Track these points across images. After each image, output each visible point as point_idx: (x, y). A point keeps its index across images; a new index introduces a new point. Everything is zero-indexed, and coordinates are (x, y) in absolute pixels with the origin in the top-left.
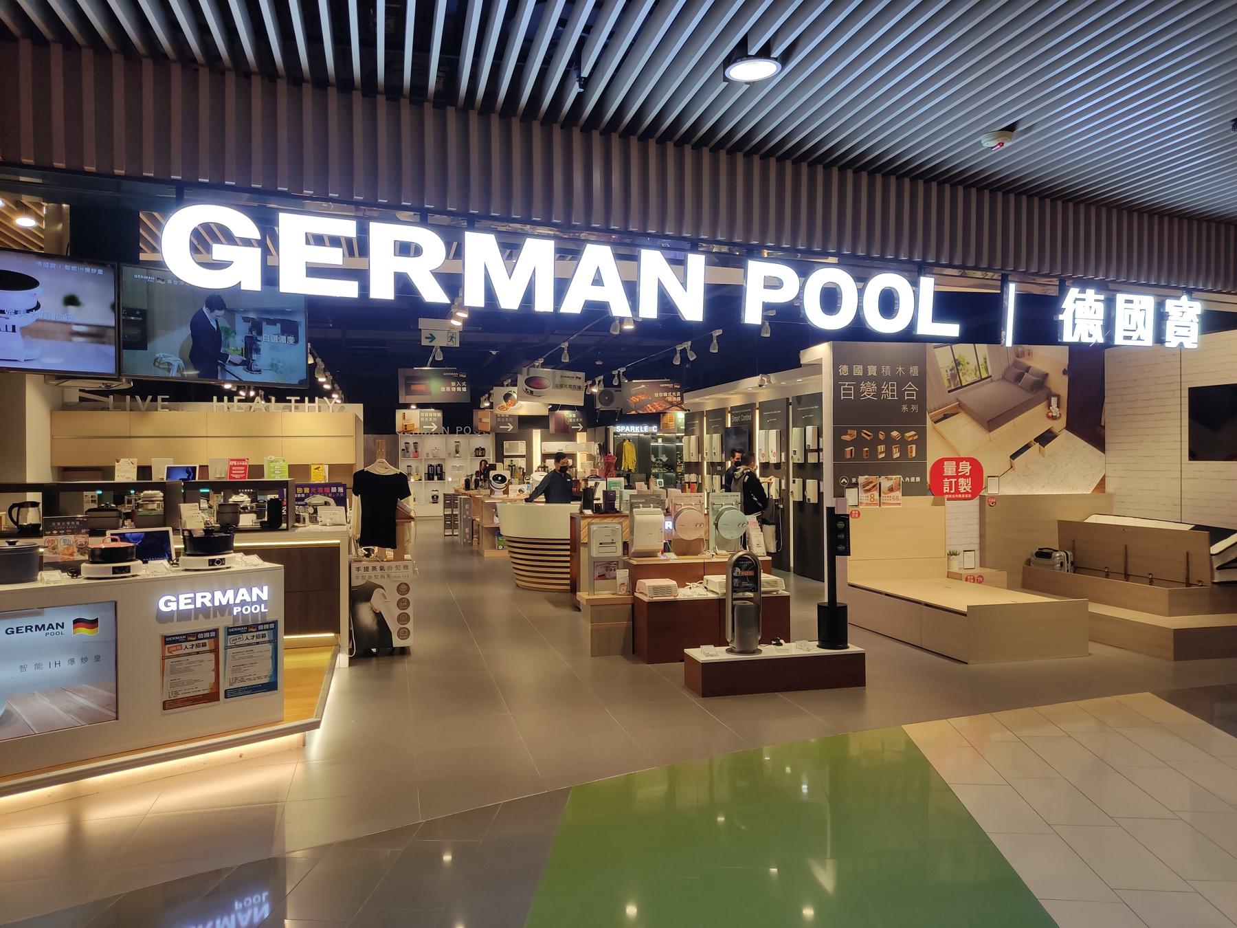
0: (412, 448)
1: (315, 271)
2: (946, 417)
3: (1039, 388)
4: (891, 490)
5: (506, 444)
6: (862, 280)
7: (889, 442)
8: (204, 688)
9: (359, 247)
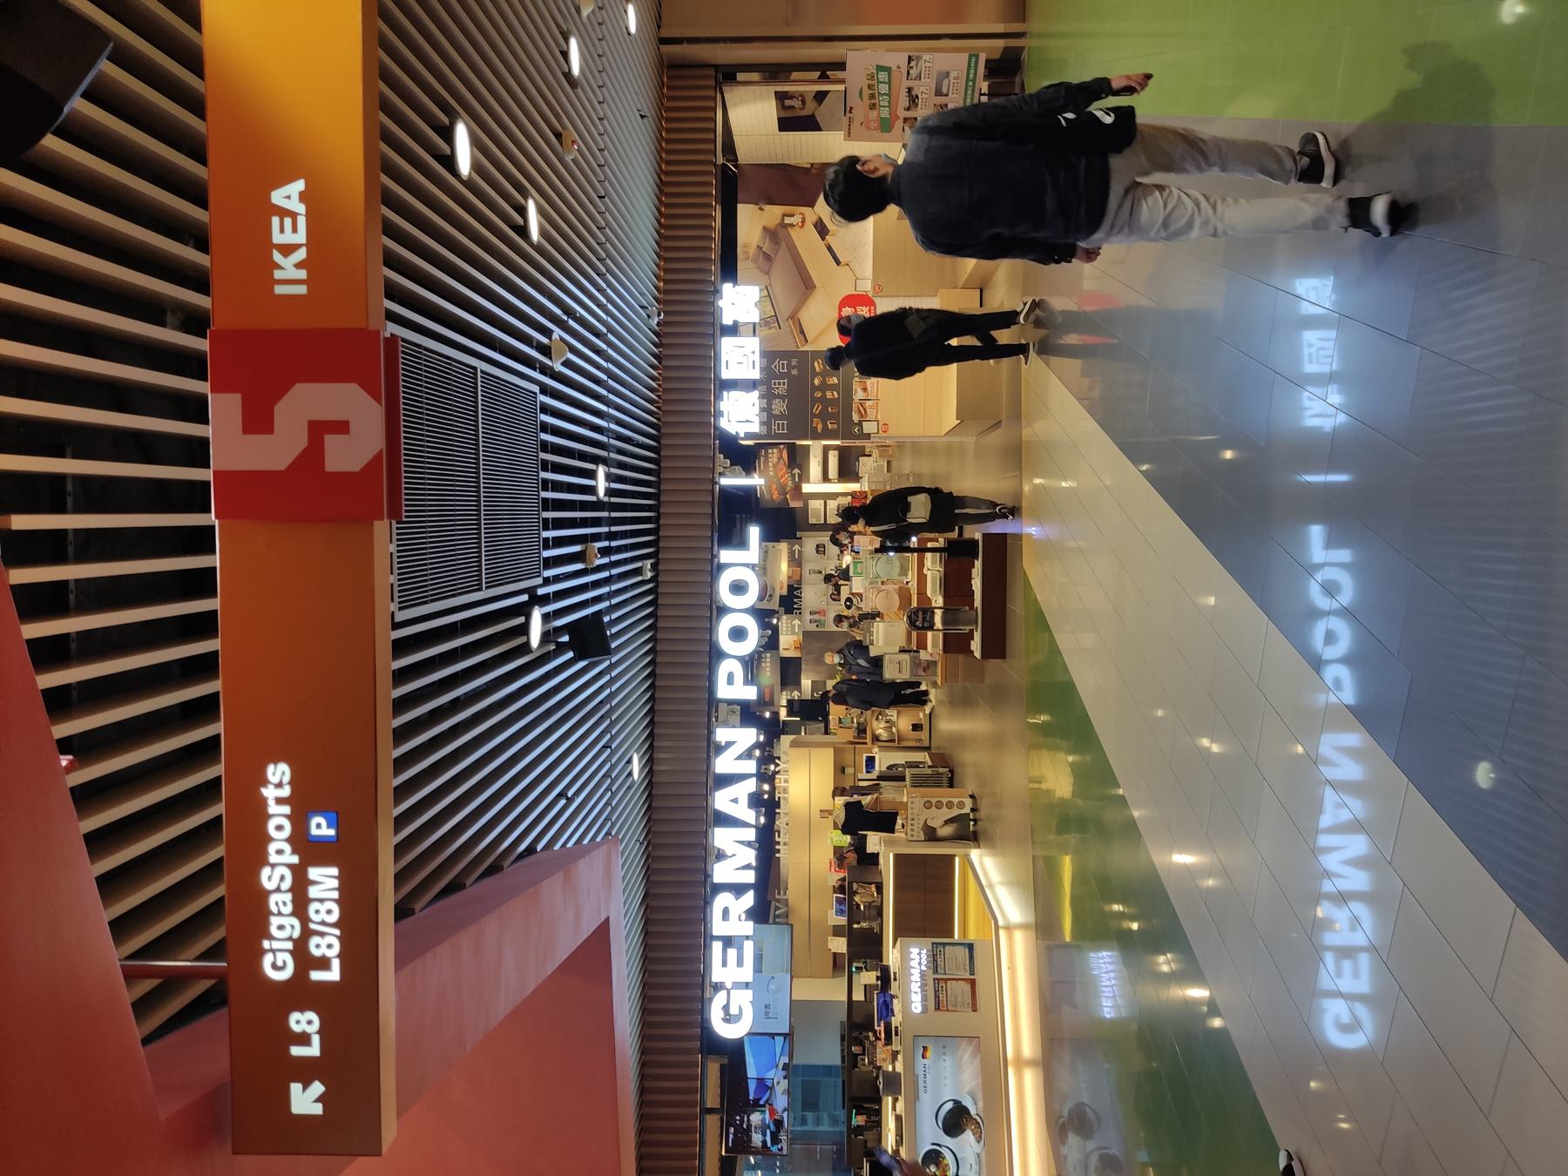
0: (816, 617)
1: (740, 963)
2: (802, 332)
3: (777, 235)
4: (865, 389)
5: (812, 521)
6: (723, 610)
7: (824, 387)
8: (967, 987)
9: (728, 941)
